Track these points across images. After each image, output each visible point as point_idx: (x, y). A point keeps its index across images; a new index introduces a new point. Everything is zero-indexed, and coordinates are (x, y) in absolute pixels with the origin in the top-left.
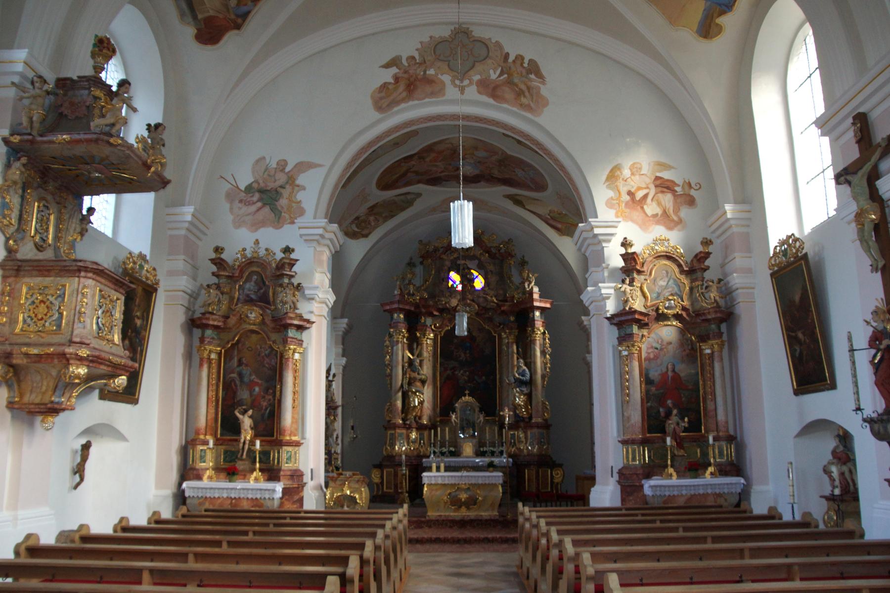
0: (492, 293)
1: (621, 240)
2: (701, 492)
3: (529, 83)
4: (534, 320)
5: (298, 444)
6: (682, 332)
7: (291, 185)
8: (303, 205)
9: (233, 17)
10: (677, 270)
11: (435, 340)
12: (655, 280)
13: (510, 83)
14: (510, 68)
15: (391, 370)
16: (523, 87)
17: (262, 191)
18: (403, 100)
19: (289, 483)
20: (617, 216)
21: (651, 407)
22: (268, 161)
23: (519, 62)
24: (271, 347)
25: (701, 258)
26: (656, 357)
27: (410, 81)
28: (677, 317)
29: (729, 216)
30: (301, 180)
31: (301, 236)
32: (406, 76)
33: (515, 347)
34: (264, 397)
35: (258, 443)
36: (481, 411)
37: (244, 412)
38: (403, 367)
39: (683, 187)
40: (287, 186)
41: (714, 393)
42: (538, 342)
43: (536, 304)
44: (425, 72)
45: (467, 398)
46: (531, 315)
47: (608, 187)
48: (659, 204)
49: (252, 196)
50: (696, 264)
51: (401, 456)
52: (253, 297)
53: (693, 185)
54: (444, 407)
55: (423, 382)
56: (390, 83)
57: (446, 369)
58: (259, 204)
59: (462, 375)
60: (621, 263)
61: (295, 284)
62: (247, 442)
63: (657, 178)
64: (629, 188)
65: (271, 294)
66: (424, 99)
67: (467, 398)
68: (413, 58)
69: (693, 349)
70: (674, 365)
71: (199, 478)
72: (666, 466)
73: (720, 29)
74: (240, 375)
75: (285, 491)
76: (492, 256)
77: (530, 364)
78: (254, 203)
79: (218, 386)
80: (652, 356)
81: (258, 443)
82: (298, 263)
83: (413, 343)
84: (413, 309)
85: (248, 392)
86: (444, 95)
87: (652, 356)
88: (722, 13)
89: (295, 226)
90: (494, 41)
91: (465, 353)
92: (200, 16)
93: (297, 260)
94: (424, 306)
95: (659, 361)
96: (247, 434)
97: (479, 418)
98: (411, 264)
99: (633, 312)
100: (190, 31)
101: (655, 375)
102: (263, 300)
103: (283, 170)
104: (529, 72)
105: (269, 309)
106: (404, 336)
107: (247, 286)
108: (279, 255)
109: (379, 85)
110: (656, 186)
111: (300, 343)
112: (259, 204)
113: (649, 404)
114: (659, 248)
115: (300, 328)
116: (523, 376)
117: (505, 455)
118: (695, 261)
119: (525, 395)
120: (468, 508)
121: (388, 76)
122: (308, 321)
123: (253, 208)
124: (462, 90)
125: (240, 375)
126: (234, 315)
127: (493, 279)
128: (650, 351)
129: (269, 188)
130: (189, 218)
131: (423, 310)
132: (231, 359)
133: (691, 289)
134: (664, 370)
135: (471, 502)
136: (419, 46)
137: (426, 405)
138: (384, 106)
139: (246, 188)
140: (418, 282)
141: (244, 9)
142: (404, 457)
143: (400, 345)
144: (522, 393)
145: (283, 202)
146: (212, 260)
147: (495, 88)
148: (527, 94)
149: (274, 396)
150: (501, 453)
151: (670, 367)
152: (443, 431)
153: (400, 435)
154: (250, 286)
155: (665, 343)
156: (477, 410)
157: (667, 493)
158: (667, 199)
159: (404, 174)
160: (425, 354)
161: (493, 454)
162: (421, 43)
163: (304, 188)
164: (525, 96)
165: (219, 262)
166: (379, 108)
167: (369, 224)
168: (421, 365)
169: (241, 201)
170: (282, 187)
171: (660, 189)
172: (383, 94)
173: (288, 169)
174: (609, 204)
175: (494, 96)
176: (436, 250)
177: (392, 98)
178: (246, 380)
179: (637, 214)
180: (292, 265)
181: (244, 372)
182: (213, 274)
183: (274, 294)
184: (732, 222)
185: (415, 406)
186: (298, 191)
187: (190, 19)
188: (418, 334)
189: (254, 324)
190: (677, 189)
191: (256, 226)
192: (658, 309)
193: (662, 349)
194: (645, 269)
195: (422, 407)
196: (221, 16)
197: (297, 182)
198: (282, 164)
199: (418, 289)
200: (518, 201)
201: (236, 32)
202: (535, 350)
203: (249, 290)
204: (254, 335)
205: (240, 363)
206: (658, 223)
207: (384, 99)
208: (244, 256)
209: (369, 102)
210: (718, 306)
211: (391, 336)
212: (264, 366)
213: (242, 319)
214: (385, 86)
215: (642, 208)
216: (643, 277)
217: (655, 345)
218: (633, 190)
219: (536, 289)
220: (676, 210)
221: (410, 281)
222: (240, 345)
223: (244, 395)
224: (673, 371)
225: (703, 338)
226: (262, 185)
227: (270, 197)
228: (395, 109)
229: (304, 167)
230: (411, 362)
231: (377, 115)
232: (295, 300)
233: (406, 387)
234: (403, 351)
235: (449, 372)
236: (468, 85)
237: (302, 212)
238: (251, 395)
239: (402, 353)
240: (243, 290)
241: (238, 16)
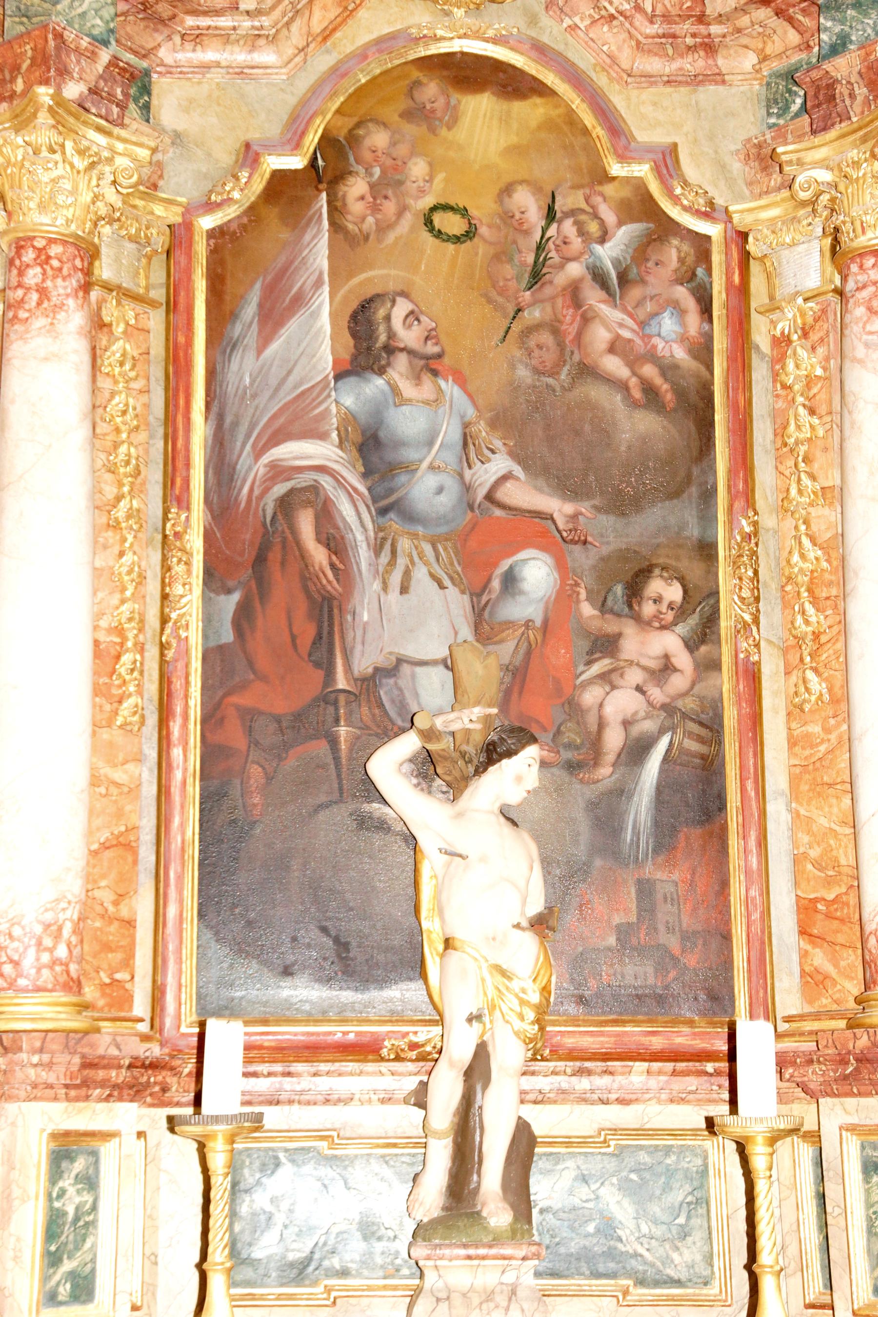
34: (606, 645)
37: (445, 770)
74: (371, 446)
85: (457, 602)
125: (371, 446)
149: (706, 632)
178: (429, 489)
181: (407, 423)
204: (479, 107)
205: (366, 346)
212: (587, 371)
222: (356, 188)
223: (409, 621)
238: (485, 627)
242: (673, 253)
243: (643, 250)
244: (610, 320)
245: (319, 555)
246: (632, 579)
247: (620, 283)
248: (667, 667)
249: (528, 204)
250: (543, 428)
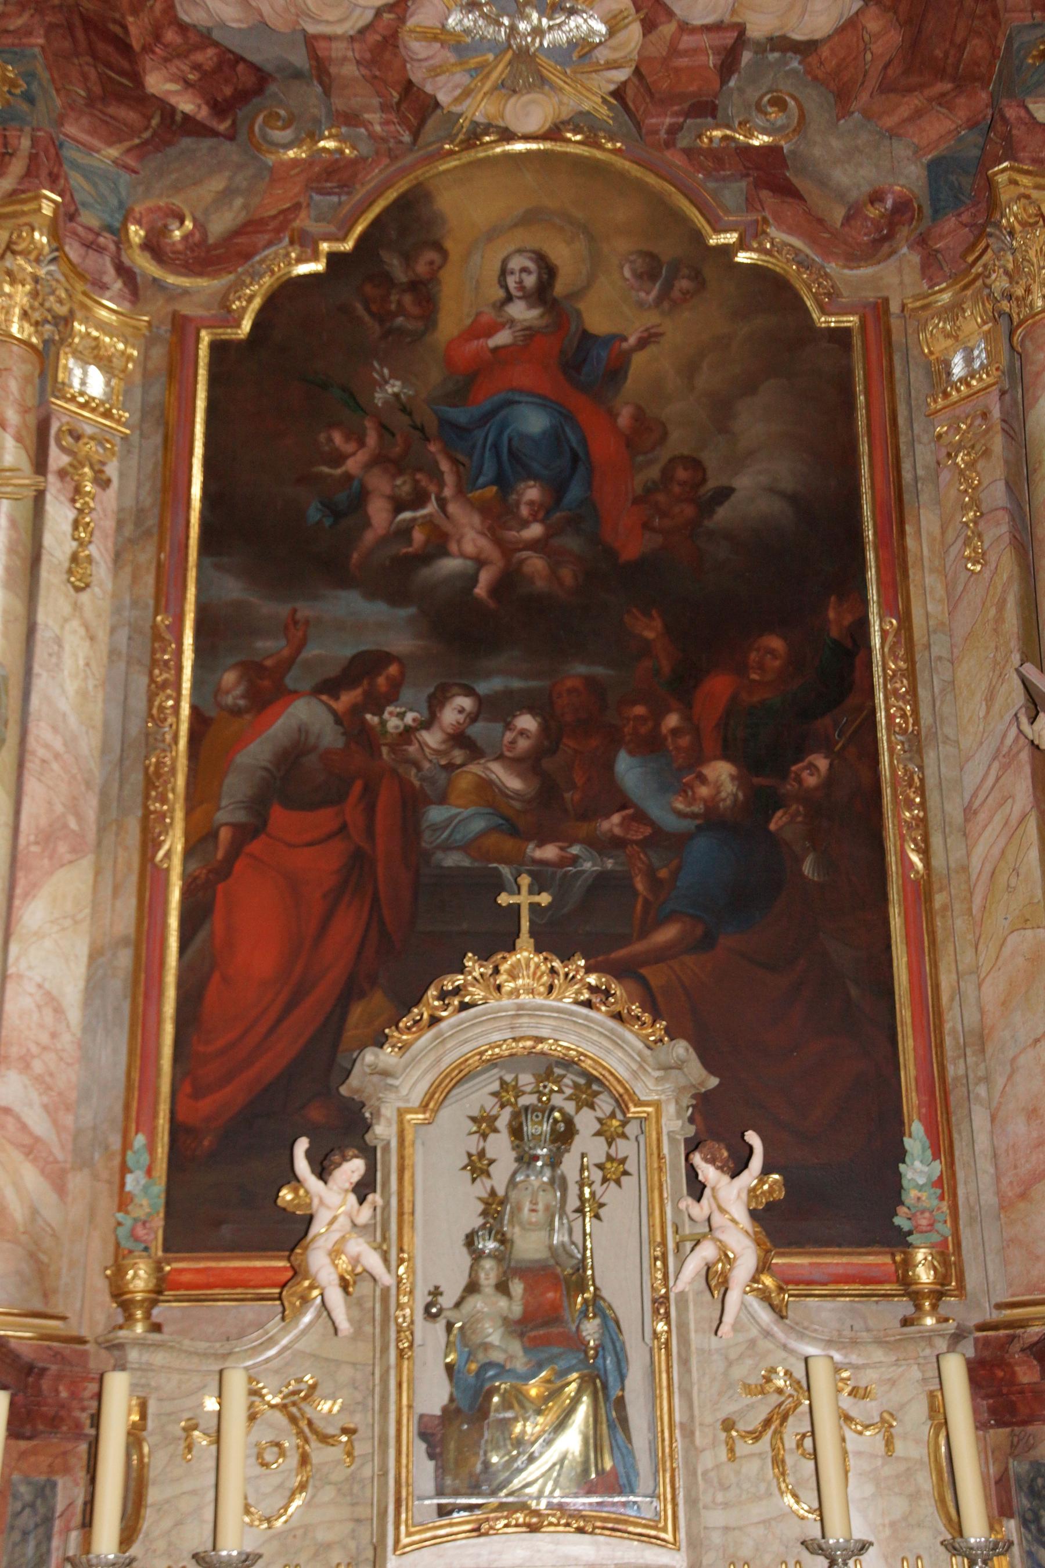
45: (528, 1003)
57: (266, 690)
67: (528, 1003)
91: (498, 516)
235: (305, 715)
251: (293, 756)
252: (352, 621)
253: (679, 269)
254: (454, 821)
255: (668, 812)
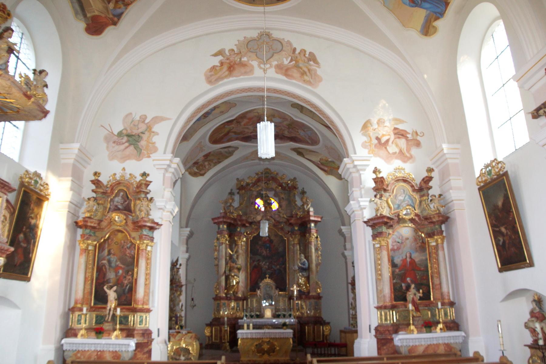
0: (283, 212)
1: (373, 169)
2: (435, 342)
3: (309, 67)
4: (310, 229)
5: (148, 311)
6: (416, 230)
7: (148, 131)
8: (157, 145)
9: (111, 16)
10: (410, 189)
11: (247, 242)
12: (396, 196)
13: (297, 66)
14: (297, 57)
15: (218, 262)
16: (306, 70)
17: (129, 136)
18: (226, 77)
19: (141, 340)
20: (369, 153)
21: (396, 283)
22: (133, 116)
23: (302, 54)
24: (131, 242)
25: (427, 180)
26: (398, 249)
27: (231, 65)
28: (412, 220)
29: (445, 151)
30: (155, 129)
31: (154, 165)
32: (228, 61)
33: (298, 247)
34: (125, 277)
35: (119, 310)
36: (277, 288)
37: (110, 288)
38: (226, 259)
39: (412, 135)
40: (146, 133)
41: (439, 273)
42: (313, 243)
43: (312, 218)
44: (240, 59)
45: (268, 280)
46: (309, 226)
47: (364, 134)
48: (397, 145)
49: (122, 139)
50: (424, 185)
51: (224, 318)
52: (120, 207)
53: (419, 133)
54: (253, 285)
55: (239, 269)
56: (217, 66)
57: (254, 261)
58: (127, 144)
59: (264, 265)
60: (373, 185)
61: (149, 198)
62: (112, 309)
63: (395, 129)
64: (377, 135)
65: (132, 205)
66: (239, 76)
67: (268, 280)
68: (233, 50)
69: (423, 243)
70: (410, 254)
71: (75, 335)
72: (409, 325)
73: (435, 29)
75: (138, 345)
76: (283, 188)
77: (308, 257)
78: (123, 144)
79: (93, 269)
80: (395, 247)
81: (119, 310)
82: (151, 184)
83: (232, 244)
84: (232, 222)
86: (253, 74)
87: (395, 247)
88: (437, 19)
89: (151, 159)
90: (286, 40)
91: (266, 251)
92: (89, 15)
93: (151, 182)
94: (240, 220)
95: (400, 251)
96: (112, 303)
97: (275, 293)
98: (231, 193)
99: (382, 217)
100: (82, 25)
101: (398, 261)
102: (127, 209)
103: (143, 122)
104: (309, 60)
105: (131, 216)
106: (226, 240)
107: (116, 199)
108: (139, 178)
109: (210, 67)
110: (395, 134)
111: (152, 239)
112: (127, 144)
113: (395, 281)
114: (398, 175)
115: (152, 229)
116: (304, 265)
117: (292, 317)
118: (423, 182)
119: (305, 277)
120: (269, 354)
121: (216, 61)
122: (157, 224)
123: (123, 147)
124: (265, 71)
125: (109, 262)
126: (106, 219)
127: (284, 203)
128: (394, 244)
129: (133, 134)
130: (76, 151)
131: (239, 223)
132: (103, 250)
133: (421, 202)
134: (404, 257)
135: (272, 350)
136: (237, 43)
137: (241, 284)
138: (213, 81)
139: (118, 133)
140: (236, 204)
141: (119, 11)
142: (226, 319)
143: (224, 245)
144: (303, 276)
145: (143, 143)
146: (93, 182)
147: (287, 70)
148: (308, 74)
149: (133, 277)
150: (290, 315)
151: (408, 255)
152: (252, 301)
153: (224, 304)
154: (118, 199)
155: (404, 239)
156: (274, 287)
157: (411, 344)
158: (402, 142)
159: (228, 133)
160: (240, 251)
161: (284, 316)
162: (238, 41)
163: (157, 134)
164: (307, 75)
165: (97, 183)
166: (210, 82)
167: (205, 167)
168: (237, 258)
169: (114, 142)
170: (143, 133)
171: (397, 136)
172: (212, 73)
173: (147, 121)
174: (364, 145)
175: (286, 75)
176: (248, 184)
177: (218, 75)
178: (113, 265)
179: (382, 152)
180: (148, 185)
181: (112, 259)
182: (93, 191)
183: (134, 205)
184: (447, 156)
185: (234, 286)
186: (153, 136)
187: (82, 17)
188: (236, 238)
189: (120, 226)
190: (408, 135)
191: (124, 159)
192: (399, 215)
193: (402, 243)
194: (389, 188)
195: (238, 285)
196: (103, 15)
197: (154, 130)
198: (143, 118)
199: (236, 209)
200: (299, 152)
201: (112, 27)
202: (311, 248)
203: (118, 202)
204: (120, 234)
205: (109, 253)
206: (397, 158)
207: (213, 76)
208: (114, 179)
209: (203, 78)
210: (440, 213)
211: (218, 239)
212: (126, 255)
213: (111, 222)
214: (214, 68)
215: (386, 148)
216: (387, 194)
217: (397, 240)
218: (379, 137)
219: (311, 209)
220: (408, 150)
221: (231, 204)
222: (110, 240)
223: (111, 275)
224: (411, 257)
225: (430, 235)
226: (129, 131)
227: (133, 140)
228: (221, 82)
229: (157, 119)
230: (231, 256)
231: (209, 87)
232: (148, 209)
233: (227, 272)
234: (226, 249)
235: (256, 263)
236: (269, 68)
237: (156, 150)
238: (116, 276)
239: (224, 250)
240: (113, 202)
241: (114, 16)
242: (133, 246)
243: (131, 246)
244: (128, 251)
245: (104, 270)
246: (127, 272)
247: (129, 248)
248: (129, 279)
249: (123, 242)
250: (122, 260)
251: (255, 265)
252: (258, 257)
253: (276, 235)
254: (264, 269)
255: (276, 269)
